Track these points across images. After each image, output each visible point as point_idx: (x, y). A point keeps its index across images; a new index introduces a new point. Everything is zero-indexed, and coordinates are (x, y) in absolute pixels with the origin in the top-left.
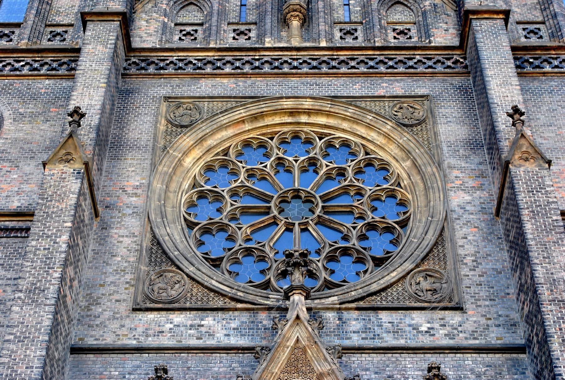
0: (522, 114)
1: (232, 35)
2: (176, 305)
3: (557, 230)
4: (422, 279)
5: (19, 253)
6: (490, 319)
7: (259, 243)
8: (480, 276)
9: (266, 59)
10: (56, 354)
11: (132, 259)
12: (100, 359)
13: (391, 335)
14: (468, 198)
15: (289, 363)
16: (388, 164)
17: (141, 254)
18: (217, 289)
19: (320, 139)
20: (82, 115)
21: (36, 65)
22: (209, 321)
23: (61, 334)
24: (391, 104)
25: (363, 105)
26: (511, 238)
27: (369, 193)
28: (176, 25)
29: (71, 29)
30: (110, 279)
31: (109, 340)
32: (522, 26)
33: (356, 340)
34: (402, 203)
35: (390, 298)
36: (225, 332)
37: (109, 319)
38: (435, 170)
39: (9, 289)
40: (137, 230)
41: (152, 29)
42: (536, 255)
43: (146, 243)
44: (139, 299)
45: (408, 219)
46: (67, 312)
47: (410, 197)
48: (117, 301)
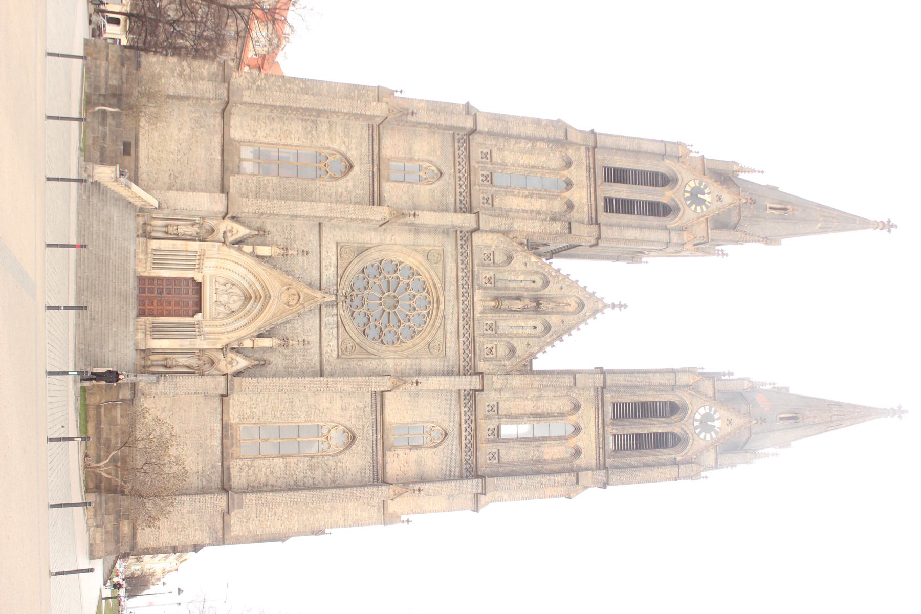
1: (488, 276)
14: (391, 367)
21: (463, 194)
22: (333, 269)
29: (490, 206)
31: (324, 235)
33: (325, 320)
39: (346, 198)
40: (374, 241)
43: (367, 246)
44: (342, 244)
47: (395, 346)
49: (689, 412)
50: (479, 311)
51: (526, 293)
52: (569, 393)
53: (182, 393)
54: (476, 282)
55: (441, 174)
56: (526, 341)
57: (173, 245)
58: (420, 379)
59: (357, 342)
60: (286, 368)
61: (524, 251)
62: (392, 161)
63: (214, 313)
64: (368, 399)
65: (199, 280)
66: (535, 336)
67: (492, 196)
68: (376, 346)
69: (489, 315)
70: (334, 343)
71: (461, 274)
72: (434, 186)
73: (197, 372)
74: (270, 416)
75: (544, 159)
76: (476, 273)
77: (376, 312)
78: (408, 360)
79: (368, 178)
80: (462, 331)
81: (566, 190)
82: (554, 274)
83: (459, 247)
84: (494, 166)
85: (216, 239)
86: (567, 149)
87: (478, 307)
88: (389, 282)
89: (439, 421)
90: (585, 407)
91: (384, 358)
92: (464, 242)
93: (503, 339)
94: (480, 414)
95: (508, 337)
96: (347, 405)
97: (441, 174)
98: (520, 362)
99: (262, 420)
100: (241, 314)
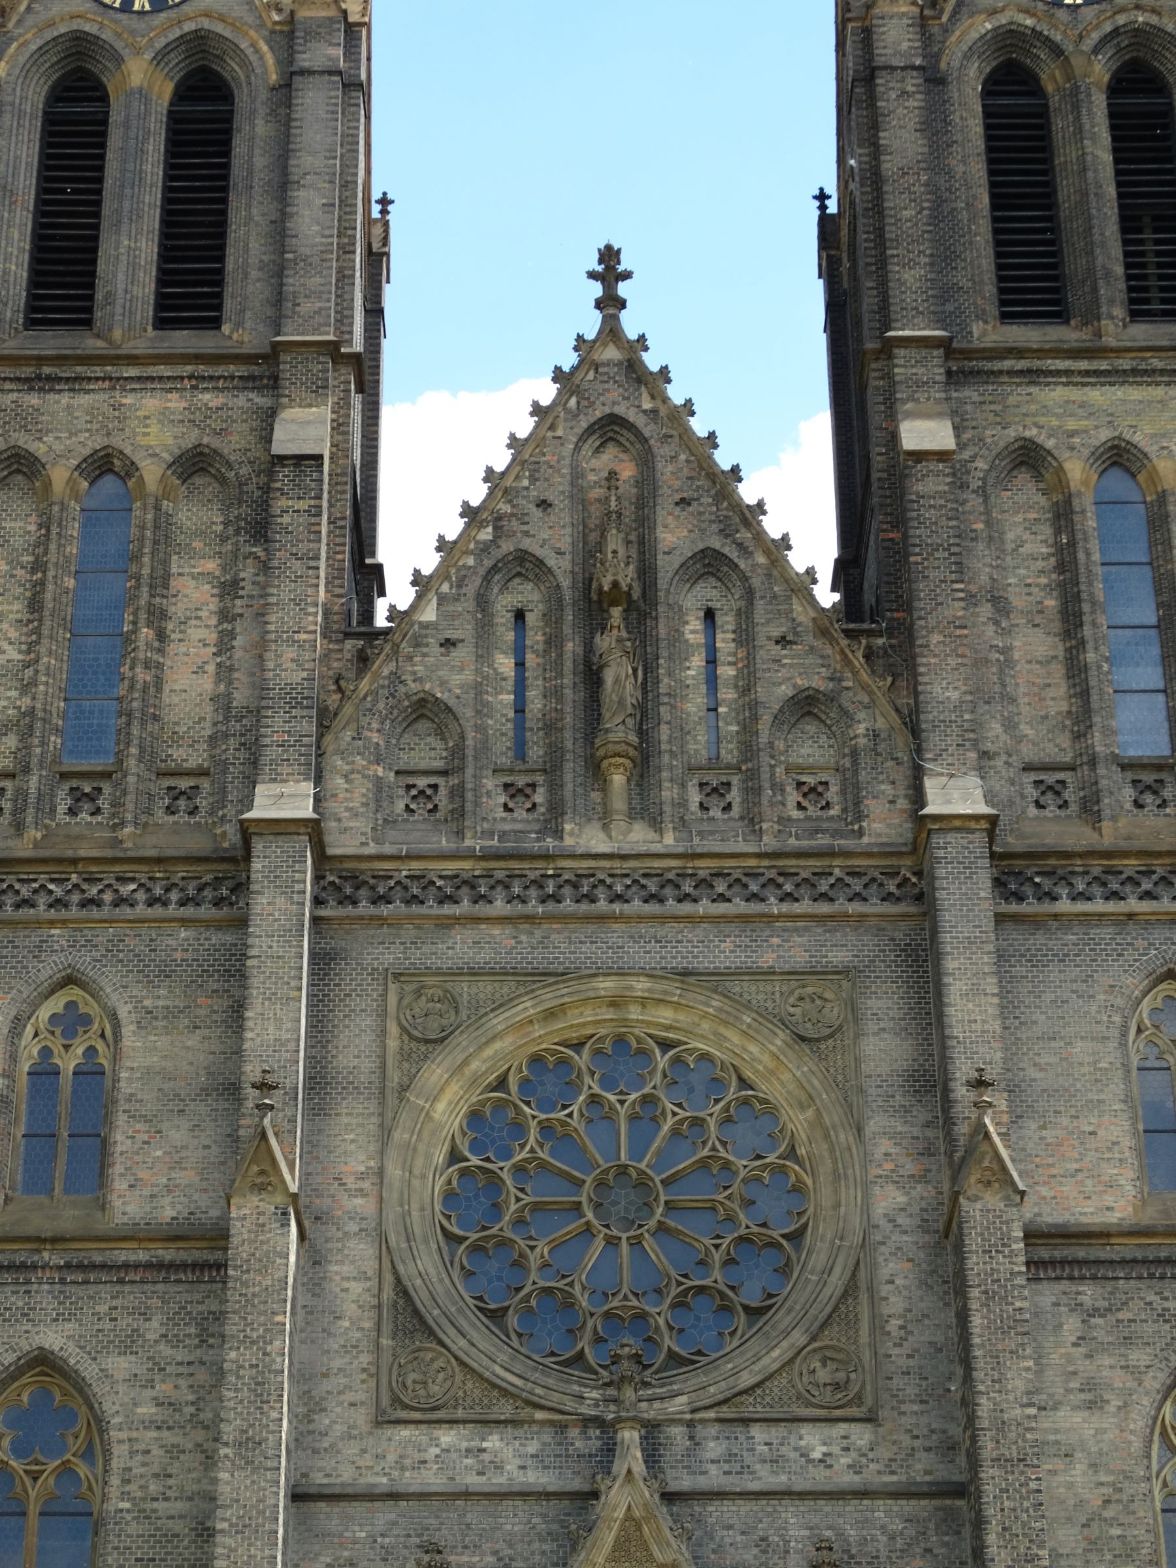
1: (502, 799)
3: (1019, 1329)
4: (818, 1364)
5: (189, 1313)
6: (917, 1437)
7: (564, 1277)
8: (909, 1356)
12: (336, 1510)
14: (902, 1199)
15: (617, 1546)
18: (504, 1385)
19: (664, 1053)
21: (158, 891)
22: (493, 1442)
24: (784, 988)
27: (743, 1173)
29: (205, 784)
30: (337, 1363)
32: (1034, 776)
33: (714, 1478)
34: (798, 1189)
35: (768, 1399)
36: (518, 1462)
37: (342, 1439)
38: (851, 1139)
39: (183, 1383)
40: (370, 1266)
43: (388, 1294)
44: (385, 1401)
45: (805, 1226)
48: (352, 1405)
49: (1029, 22)
50: (652, 835)
52: (975, 484)
54: (532, 844)
56: (767, 650)
58: (962, 1070)
59: (803, 1340)
61: (396, 647)
64: (1048, 1294)
66: (745, 615)
67: (161, 774)
68: (818, 1260)
69: (668, 793)
72: (123, 1011)
76: (495, 842)
79: (92, 1290)
80: (739, 906)
81: (129, 475)
82: (486, 534)
83: (385, 910)
84: (35, 761)
87: (639, 837)
88: (536, 1207)
89: (1120, 1002)
90: (1029, 421)
91: (870, 1226)
92: (363, 892)
93: (764, 739)
94: (1078, 836)
95: (755, 718)
96: (1074, 1385)
97: (69, 980)
98: (855, 673)
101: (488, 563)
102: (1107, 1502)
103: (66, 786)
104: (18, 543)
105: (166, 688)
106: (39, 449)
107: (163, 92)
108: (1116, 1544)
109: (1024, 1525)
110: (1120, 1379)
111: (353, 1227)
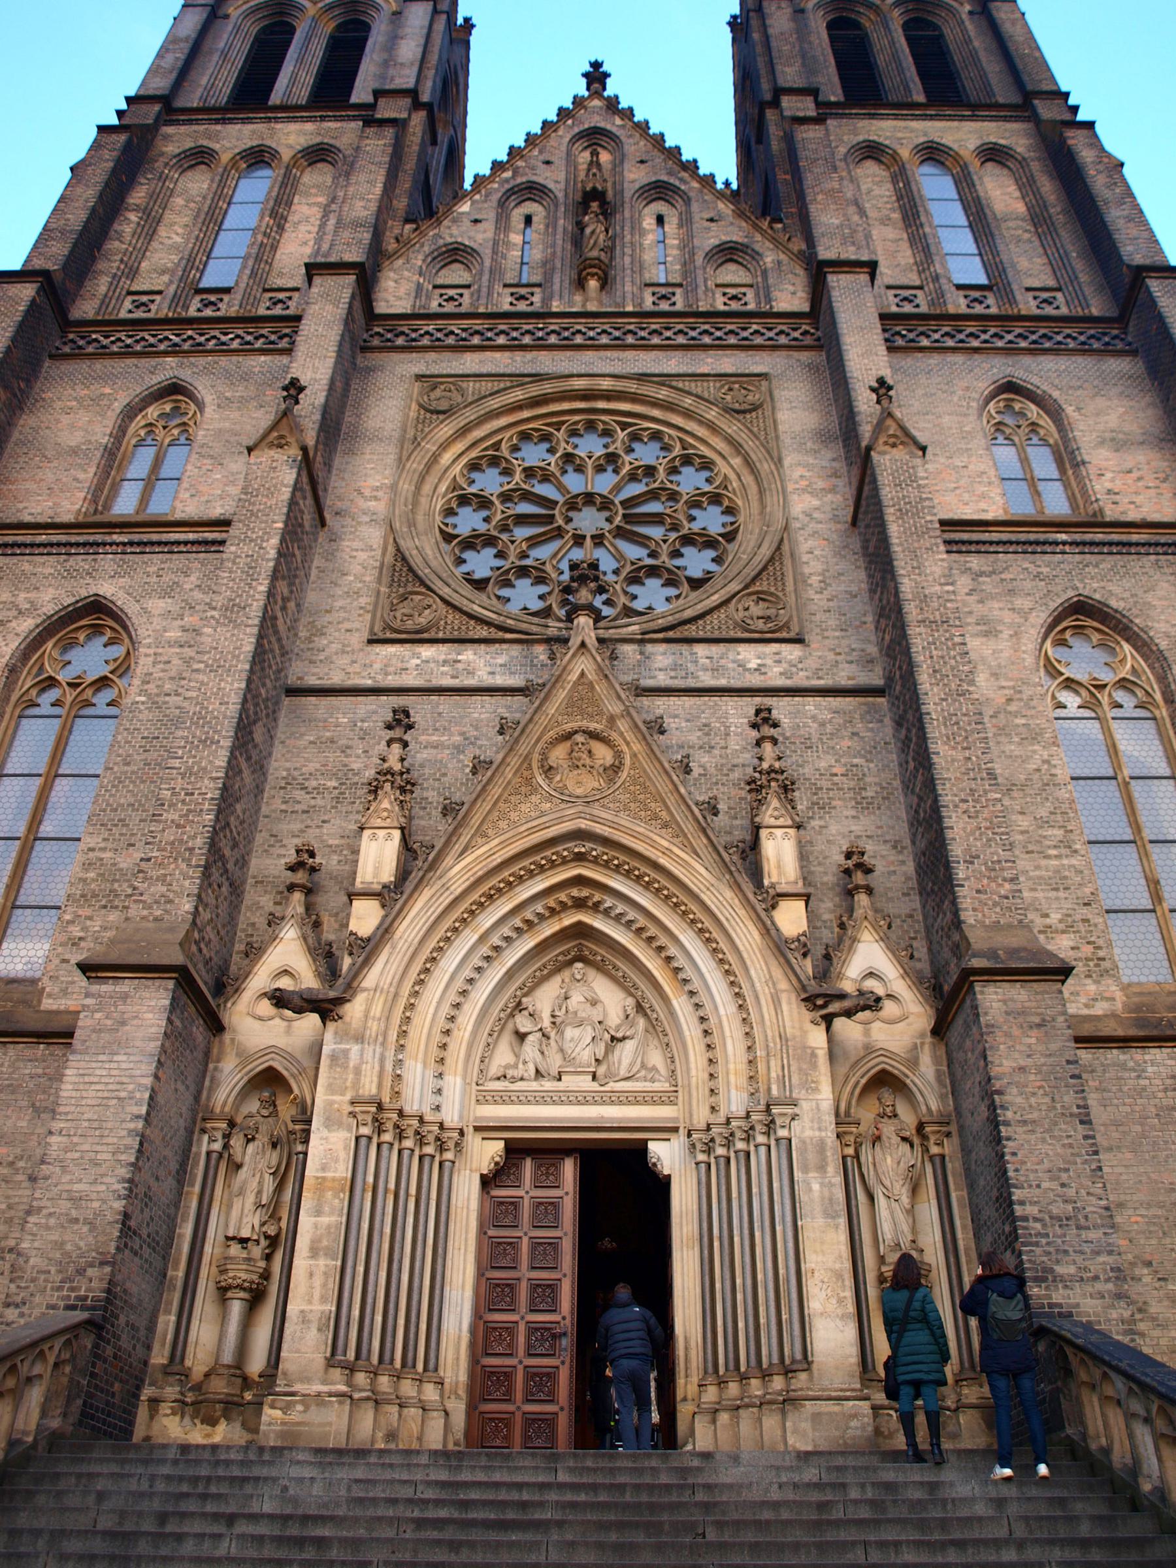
0: (890, 388)
2: (426, 636)
9: (552, 327)
10: (263, 691)
11: (368, 579)
13: (709, 673)
14: (816, 502)
16: (713, 463)
17: (381, 572)
20: (301, 389)
21: (249, 338)
22: (468, 654)
23: (270, 667)
25: (680, 385)
26: (871, 550)
27: (685, 498)
28: (435, 287)
29: (296, 295)
33: (662, 680)
36: (489, 669)
41: (402, 291)
42: (902, 564)
43: (389, 558)
45: (736, 531)
46: (279, 640)
47: (740, 503)
51: (561, 222)
53: (1097, 1189)
55: (175, 389)
56: (699, 223)
57: (314, 1252)
60: (863, 805)
62: (107, 507)
63: (648, 1086)
65: (488, 1152)
67: (266, 290)
70: (750, 655)
71: (501, 340)
73: (935, 1150)
74: (1065, 862)
75: (179, 201)
77: (633, 552)
78: (787, 462)
85: (307, 1063)
86: (162, 154)
99: (1087, 891)
100: (653, 964)
101: (507, 186)
102: (1009, 700)
103: (198, 298)
104: (194, 193)
105: (279, 253)
106: (216, 147)
107: (328, 28)
108: (1021, 729)
109: (953, 668)
110: (1008, 616)
111: (367, 519)
